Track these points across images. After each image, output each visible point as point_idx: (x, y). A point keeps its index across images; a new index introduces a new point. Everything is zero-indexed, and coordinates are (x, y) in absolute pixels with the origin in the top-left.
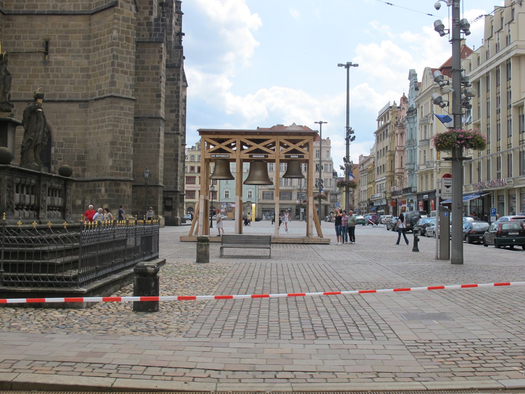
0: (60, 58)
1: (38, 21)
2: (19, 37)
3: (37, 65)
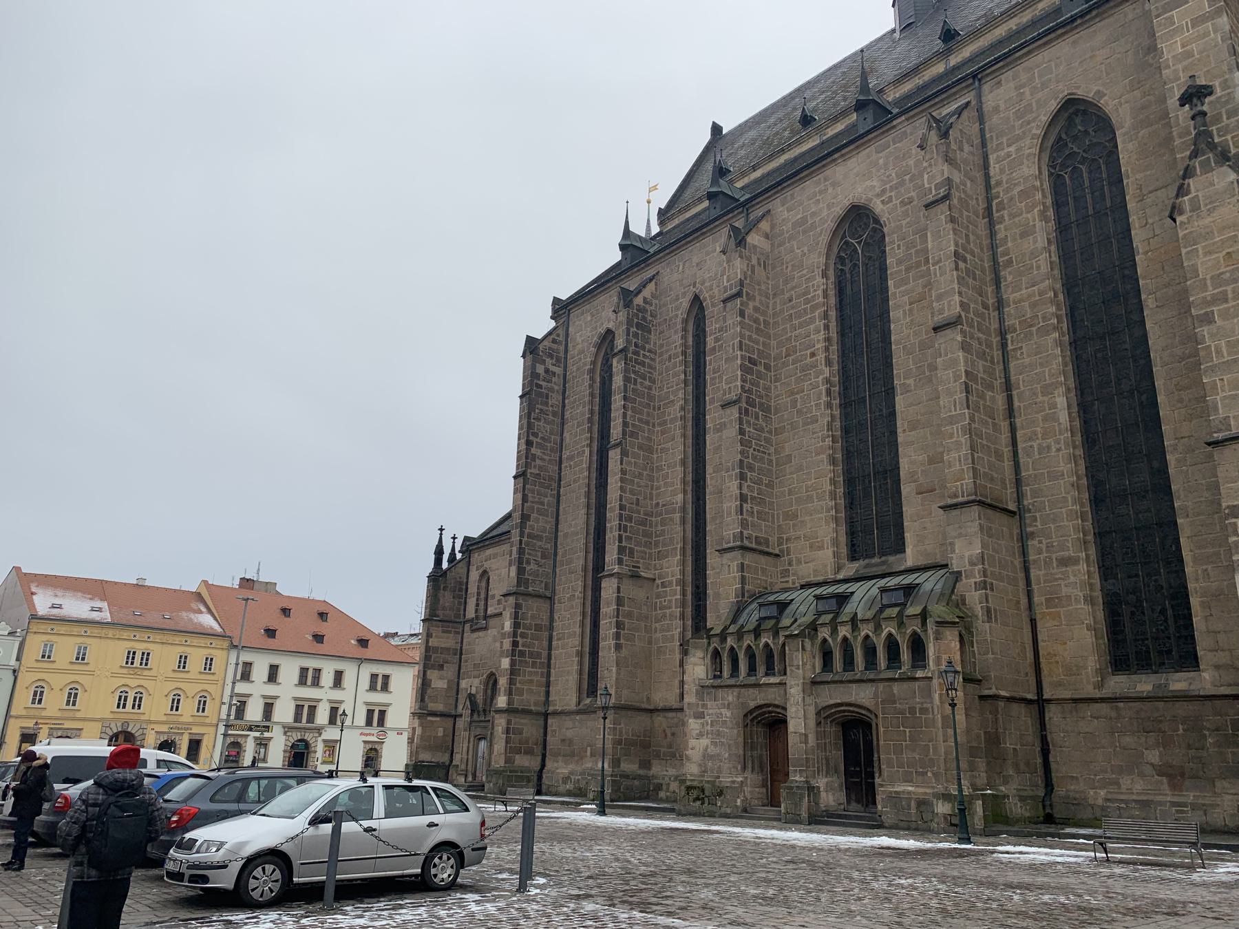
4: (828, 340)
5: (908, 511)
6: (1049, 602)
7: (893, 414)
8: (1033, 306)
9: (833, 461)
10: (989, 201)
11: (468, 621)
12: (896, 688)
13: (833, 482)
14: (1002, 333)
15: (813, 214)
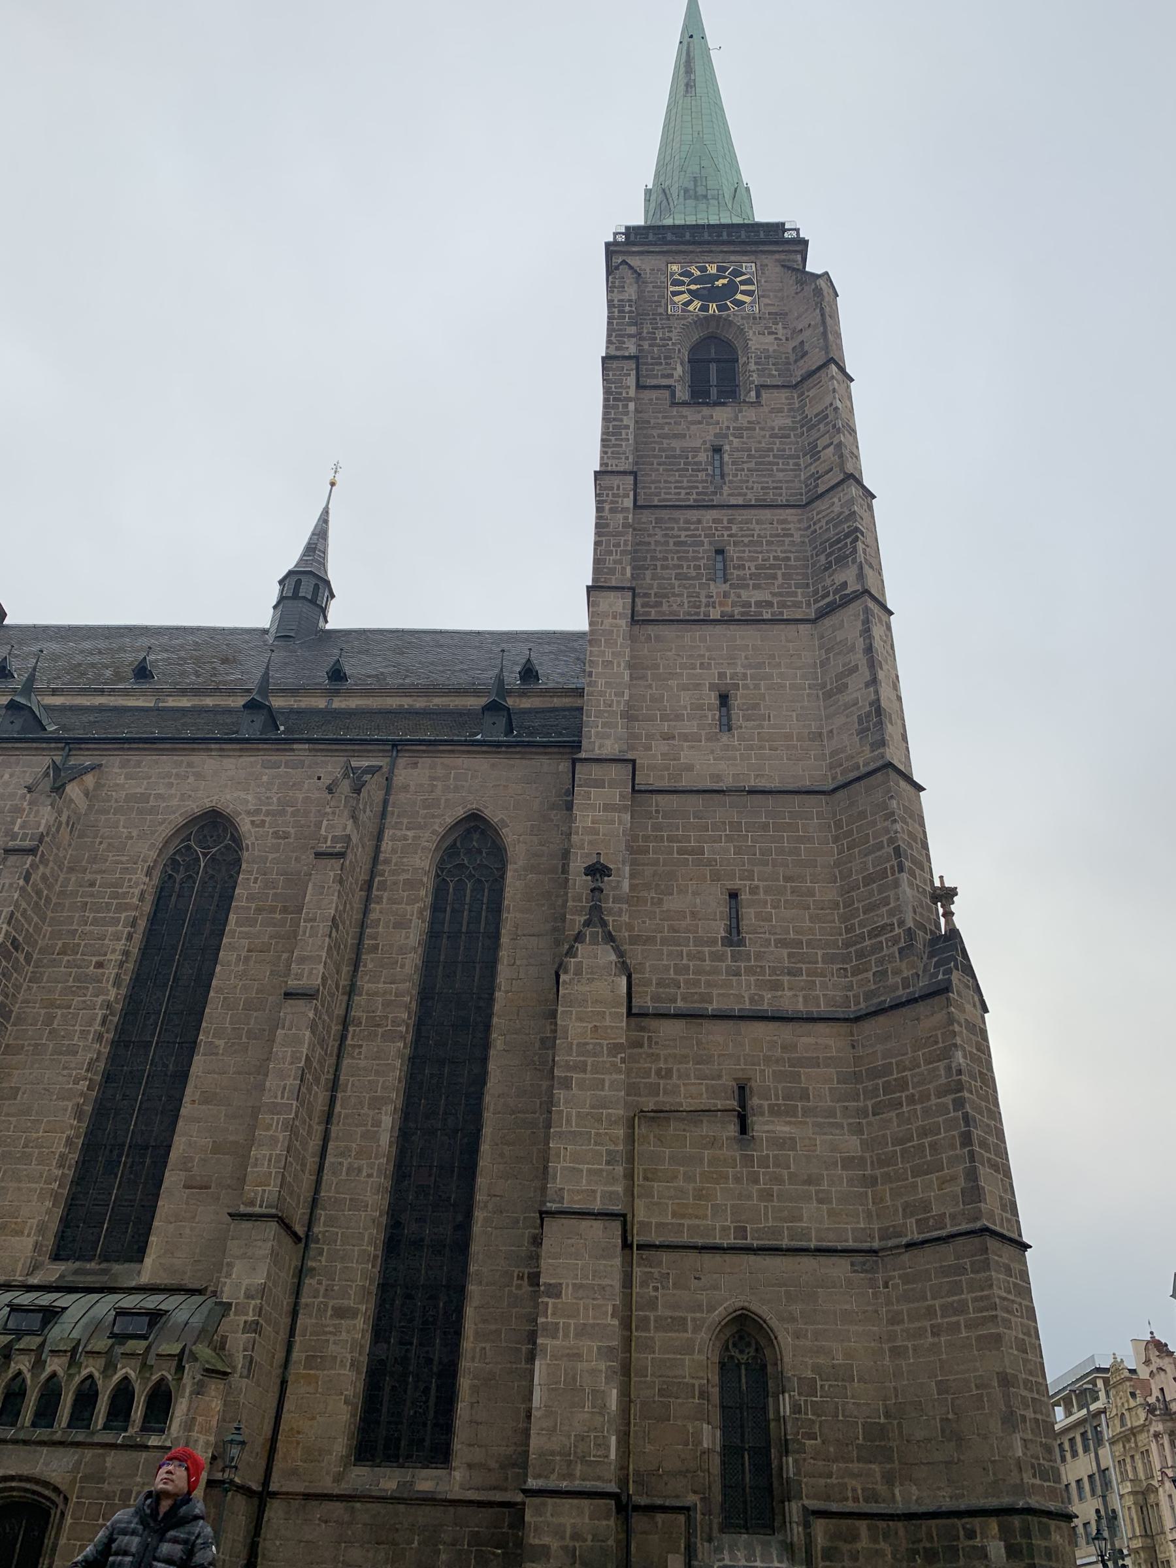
0: (782, 1128)
1: (717, 1035)
2: (669, 1072)
3: (721, 1148)
4: (126, 953)
5: (165, 1206)
6: (310, 1362)
7: (183, 1076)
8: (387, 1004)
9: (79, 1114)
10: (372, 874)
12: (112, 1459)
13: (69, 1142)
14: (345, 1022)
15: (159, 796)
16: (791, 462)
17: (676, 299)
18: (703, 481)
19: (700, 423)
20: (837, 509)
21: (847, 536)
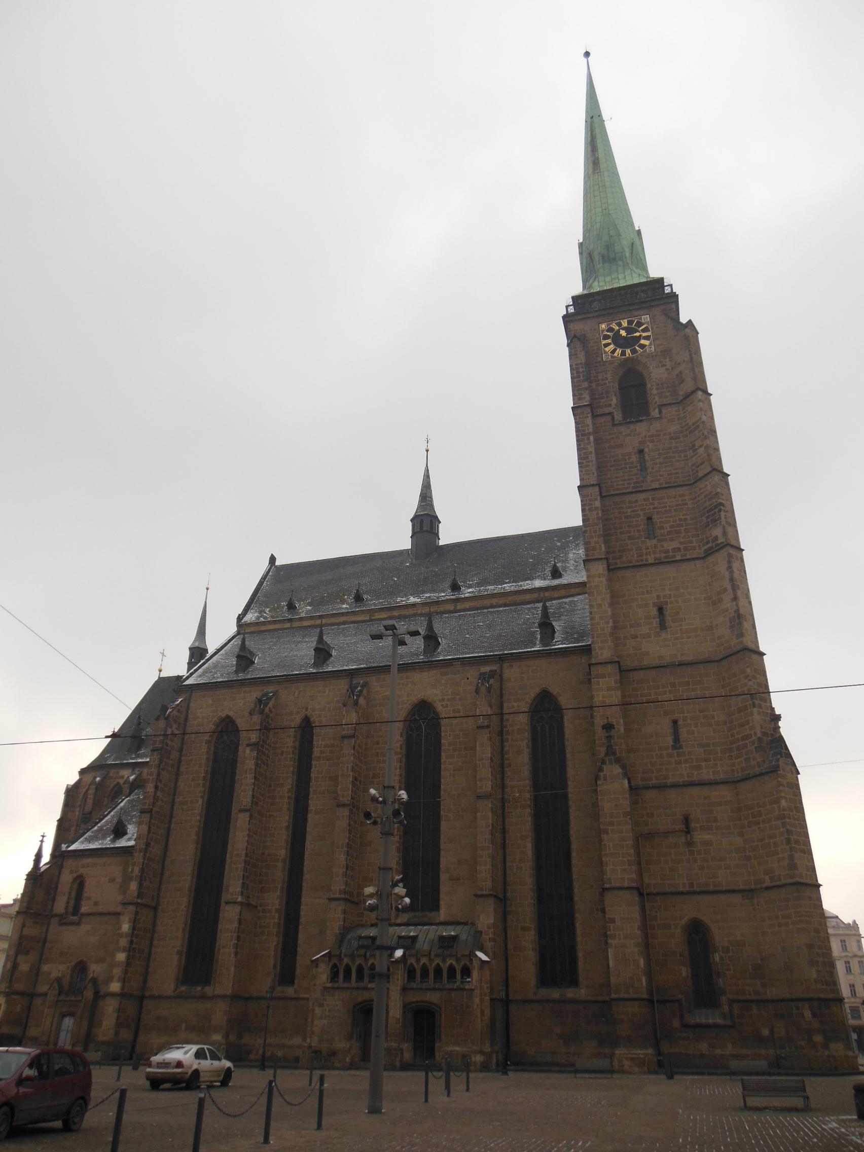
0: (707, 837)
7: (437, 830)
11: (56, 915)
16: (683, 455)
17: (607, 349)
18: (636, 474)
19: (630, 435)
20: (709, 488)
21: (716, 507)
